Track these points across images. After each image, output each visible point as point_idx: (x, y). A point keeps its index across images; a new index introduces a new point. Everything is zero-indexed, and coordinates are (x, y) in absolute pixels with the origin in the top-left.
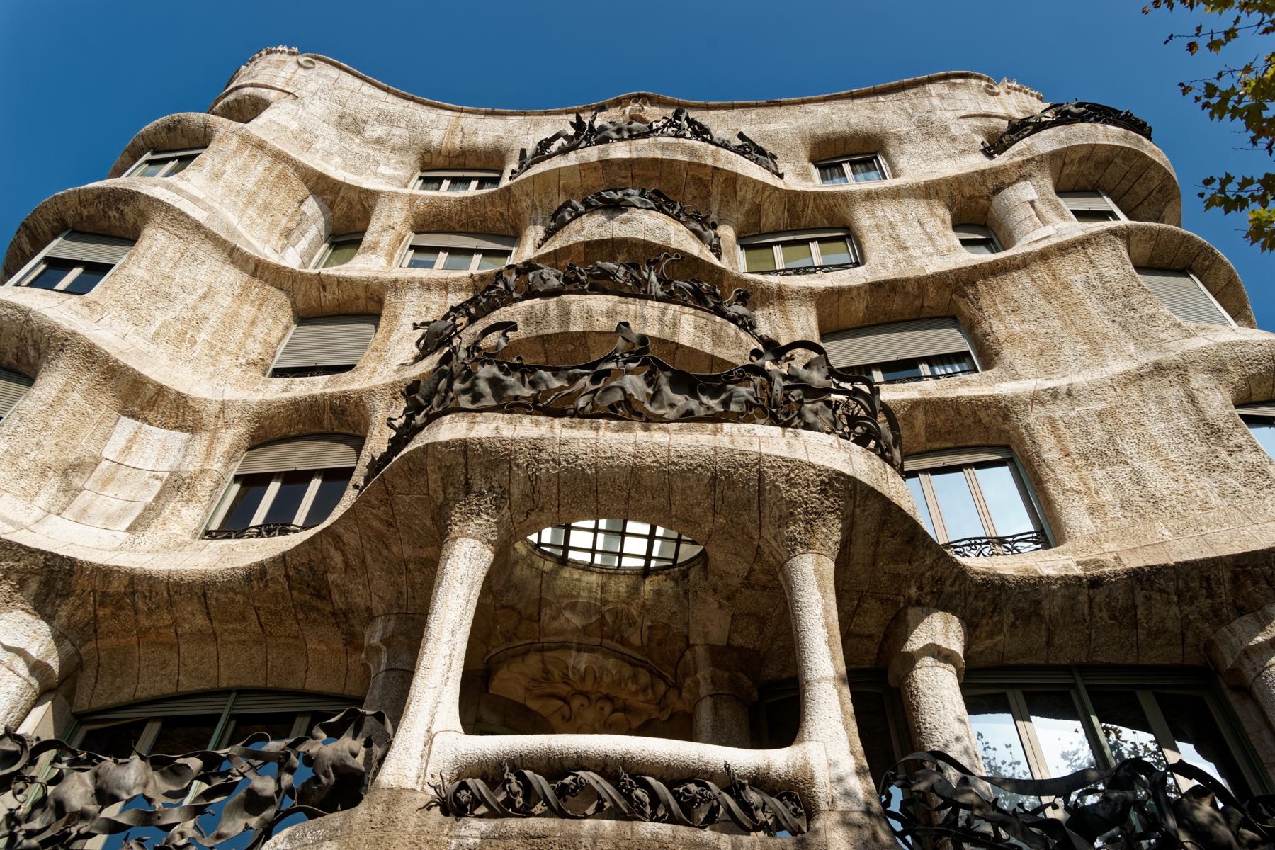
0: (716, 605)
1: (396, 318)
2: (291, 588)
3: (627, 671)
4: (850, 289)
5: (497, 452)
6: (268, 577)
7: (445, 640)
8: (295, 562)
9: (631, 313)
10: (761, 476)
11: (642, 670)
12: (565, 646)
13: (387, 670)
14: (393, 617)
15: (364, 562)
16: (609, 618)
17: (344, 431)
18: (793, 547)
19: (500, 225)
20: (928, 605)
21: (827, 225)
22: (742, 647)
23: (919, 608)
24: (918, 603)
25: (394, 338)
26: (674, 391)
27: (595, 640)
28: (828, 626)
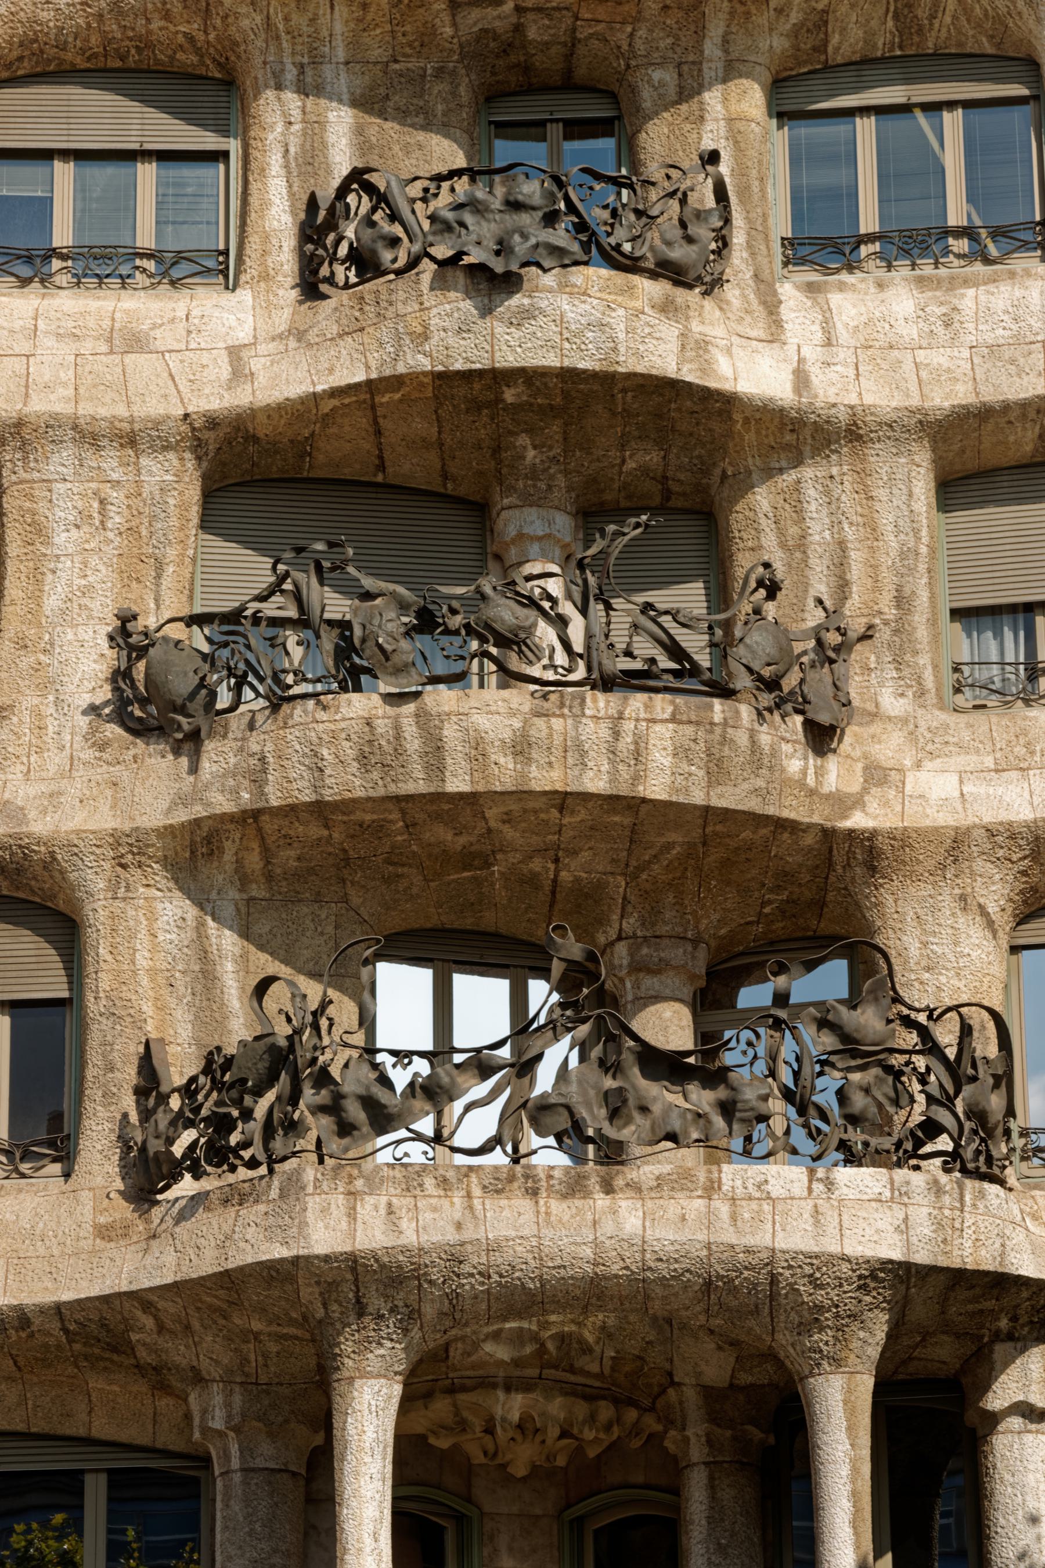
0: (713, 1346)
1: (38, 531)
2: (70, 1342)
3: (581, 1409)
4: (1006, 407)
5: (400, 1267)
6: (34, 1328)
7: (368, 1550)
8: (77, 1316)
9: (558, 740)
10: (774, 1279)
11: (603, 1403)
12: (486, 1384)
13: (242, 1470)
14: (237, 1388)
15: (188, 1327)
16: (550, 1346)
17: (21, 895)
18: (817, 1359)
19: (187, 59)
20: (1024, 1338)
21: (990, 50)
22: (752, 1385)
23: (1011, 1344)
24: (1010, 1337)
25: (52, 603)
26: (645, 1075)
27: (532, 1372)
28: (855, 1494)
